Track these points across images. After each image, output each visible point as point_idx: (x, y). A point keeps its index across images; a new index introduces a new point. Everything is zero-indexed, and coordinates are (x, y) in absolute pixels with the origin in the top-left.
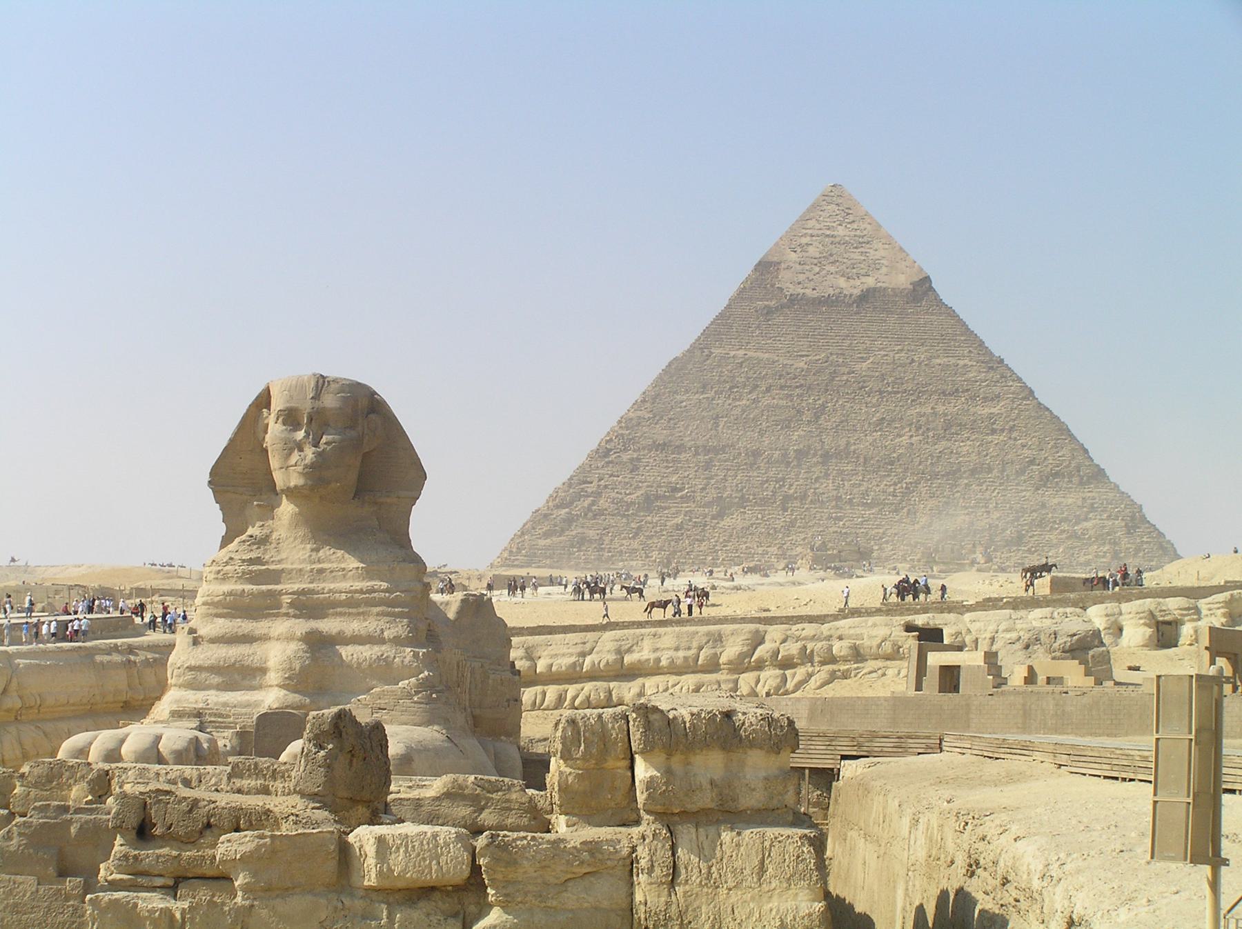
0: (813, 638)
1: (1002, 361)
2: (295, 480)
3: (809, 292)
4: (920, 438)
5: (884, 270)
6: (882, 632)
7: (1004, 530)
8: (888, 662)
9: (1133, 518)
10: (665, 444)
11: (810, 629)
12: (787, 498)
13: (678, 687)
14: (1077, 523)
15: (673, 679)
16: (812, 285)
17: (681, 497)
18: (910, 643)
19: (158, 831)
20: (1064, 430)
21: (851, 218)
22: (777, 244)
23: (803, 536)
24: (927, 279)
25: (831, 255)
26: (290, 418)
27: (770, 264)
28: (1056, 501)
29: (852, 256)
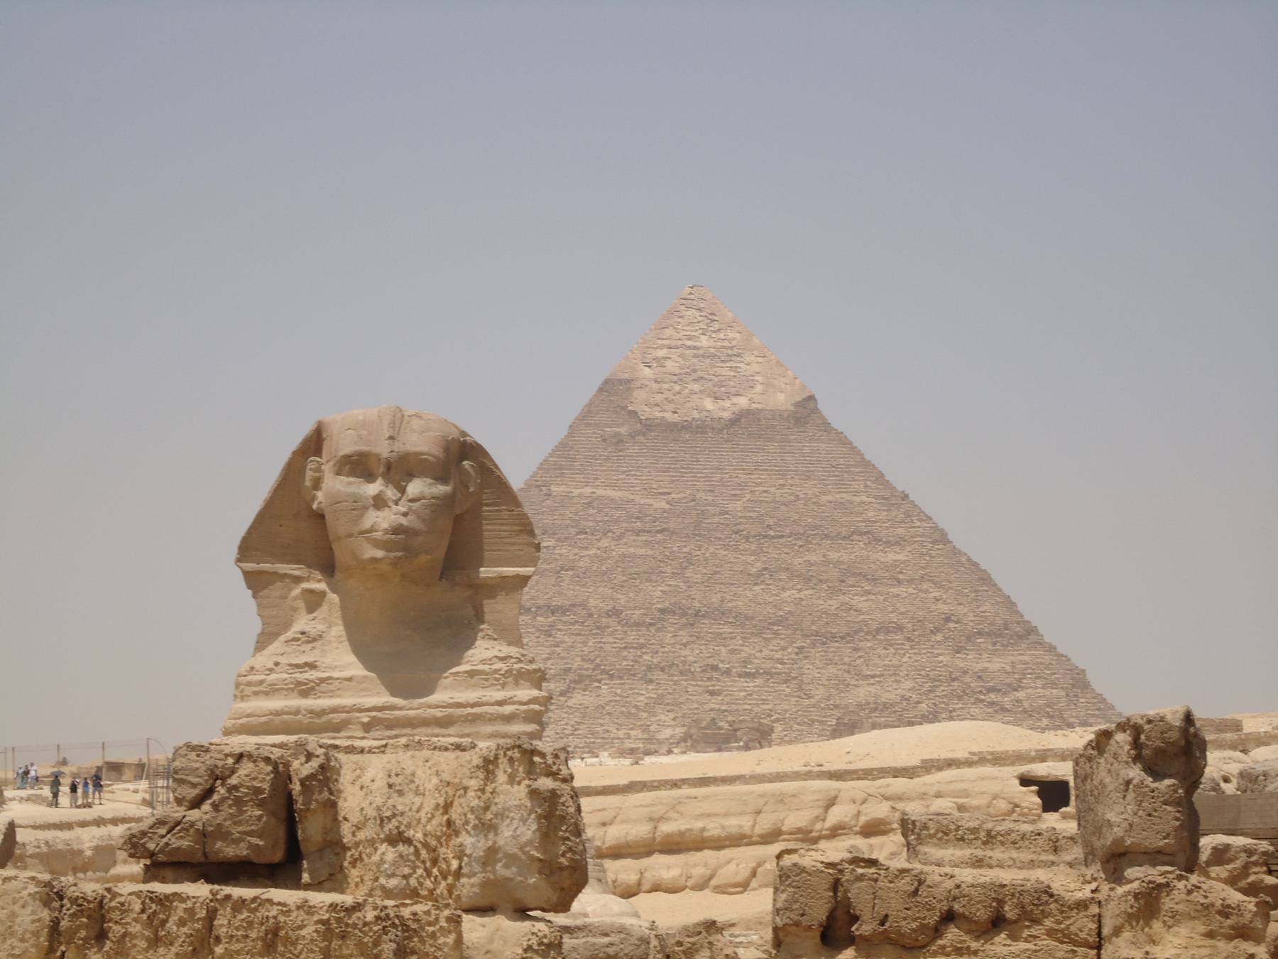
0: (899, 798)
1: (905, 497)
3: (668, 415)
4: (810, 592)
5: (759, 388)
6: (994, 788)
7: (918, 703)
9: (1073, 685)
12: (649, 668)
13: (732, 866)
14: (1005, 693)
16: (671, 407)
18: (1031, 798)
19: (865, 928)
20: (985, 579)
21: (716, 326)
24: (811, 398)
25: (695, 371)
26: (359, 465)
27: (621, 382)
28: (978, 667)
29: (719, 371)
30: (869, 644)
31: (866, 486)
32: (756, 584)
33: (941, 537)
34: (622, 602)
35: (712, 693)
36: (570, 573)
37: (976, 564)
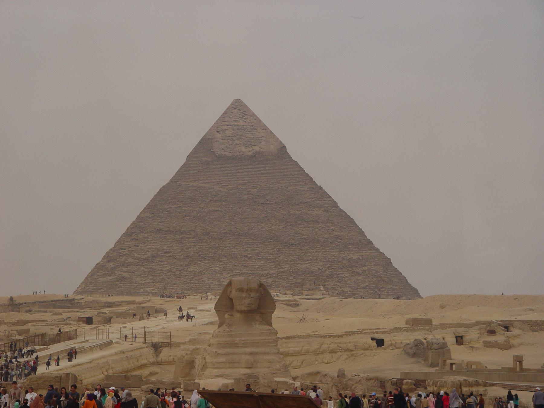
0: (340, 343)
1: (321, 188)
2: (244, 308)
3: (227, 153)
5: (263, 143)
8: (368, 351)
10: (160, 230)
11: (339, 340)
15: (294, 358)
17: (170, 256)
18: (374, 344)
20: (352, 221)
22: (210, 129)
23: (229, 275)
24: (283, 148)
25: (238, 135)
26: (241, 290)
30: (306, 248)
31: (306, 184)
32: (262, 223)
33: (335, 204)
34: (209, 229)
35: (244, 266)
36: (189, 217)
37: (349, 216)
